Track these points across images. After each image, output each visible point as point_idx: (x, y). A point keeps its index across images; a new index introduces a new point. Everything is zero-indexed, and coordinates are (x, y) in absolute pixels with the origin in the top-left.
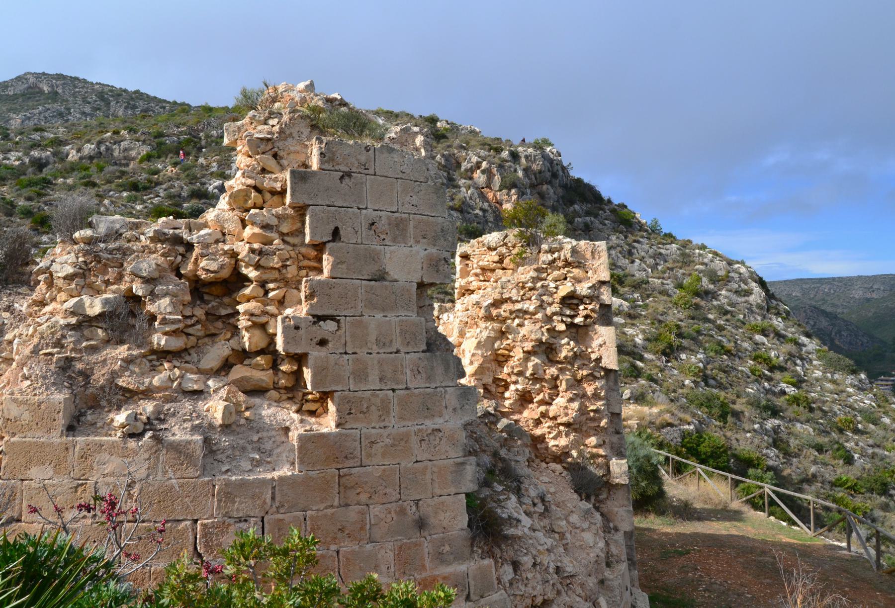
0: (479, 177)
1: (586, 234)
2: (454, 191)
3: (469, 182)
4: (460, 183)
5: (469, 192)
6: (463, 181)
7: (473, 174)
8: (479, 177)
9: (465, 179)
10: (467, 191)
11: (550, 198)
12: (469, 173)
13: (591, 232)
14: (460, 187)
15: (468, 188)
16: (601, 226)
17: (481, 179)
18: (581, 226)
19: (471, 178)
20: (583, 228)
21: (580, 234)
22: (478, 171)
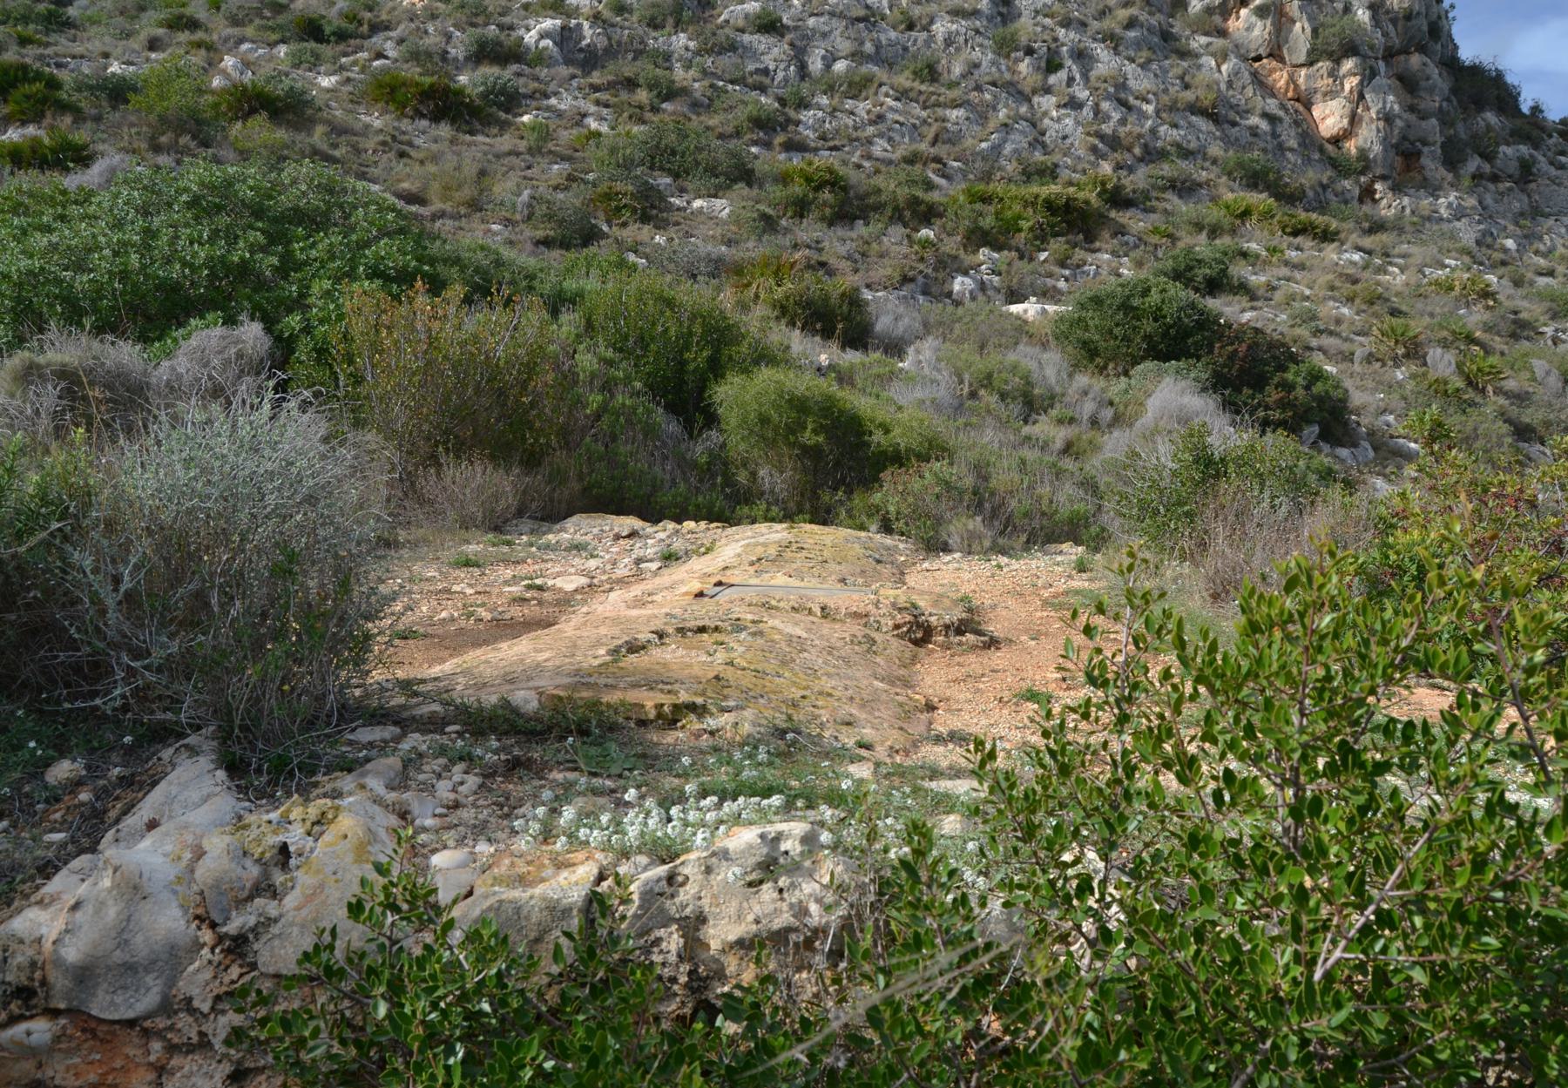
0: (1249, 29)
1: (1522, 191)
2: (1185, 64)
3: (1218, 43)
4: (1194, 45)
5: (1224, 68)
6: (1203, 40)
7: (1226, 20)
8: (1249, 29)
9: (1206, 34)
10: (1219, 66)
11: (1431, 90)
12: (1217, 19)
13: (1533, 186)
14: (1197, 56)
15: (1222, 57)
16: (1553, 171)
17: (1257, 32)
18: (1513, 168)
19: (1222, 33)
20: (1517, 173)
21: (1510, 189)
22: (1244, 12)
